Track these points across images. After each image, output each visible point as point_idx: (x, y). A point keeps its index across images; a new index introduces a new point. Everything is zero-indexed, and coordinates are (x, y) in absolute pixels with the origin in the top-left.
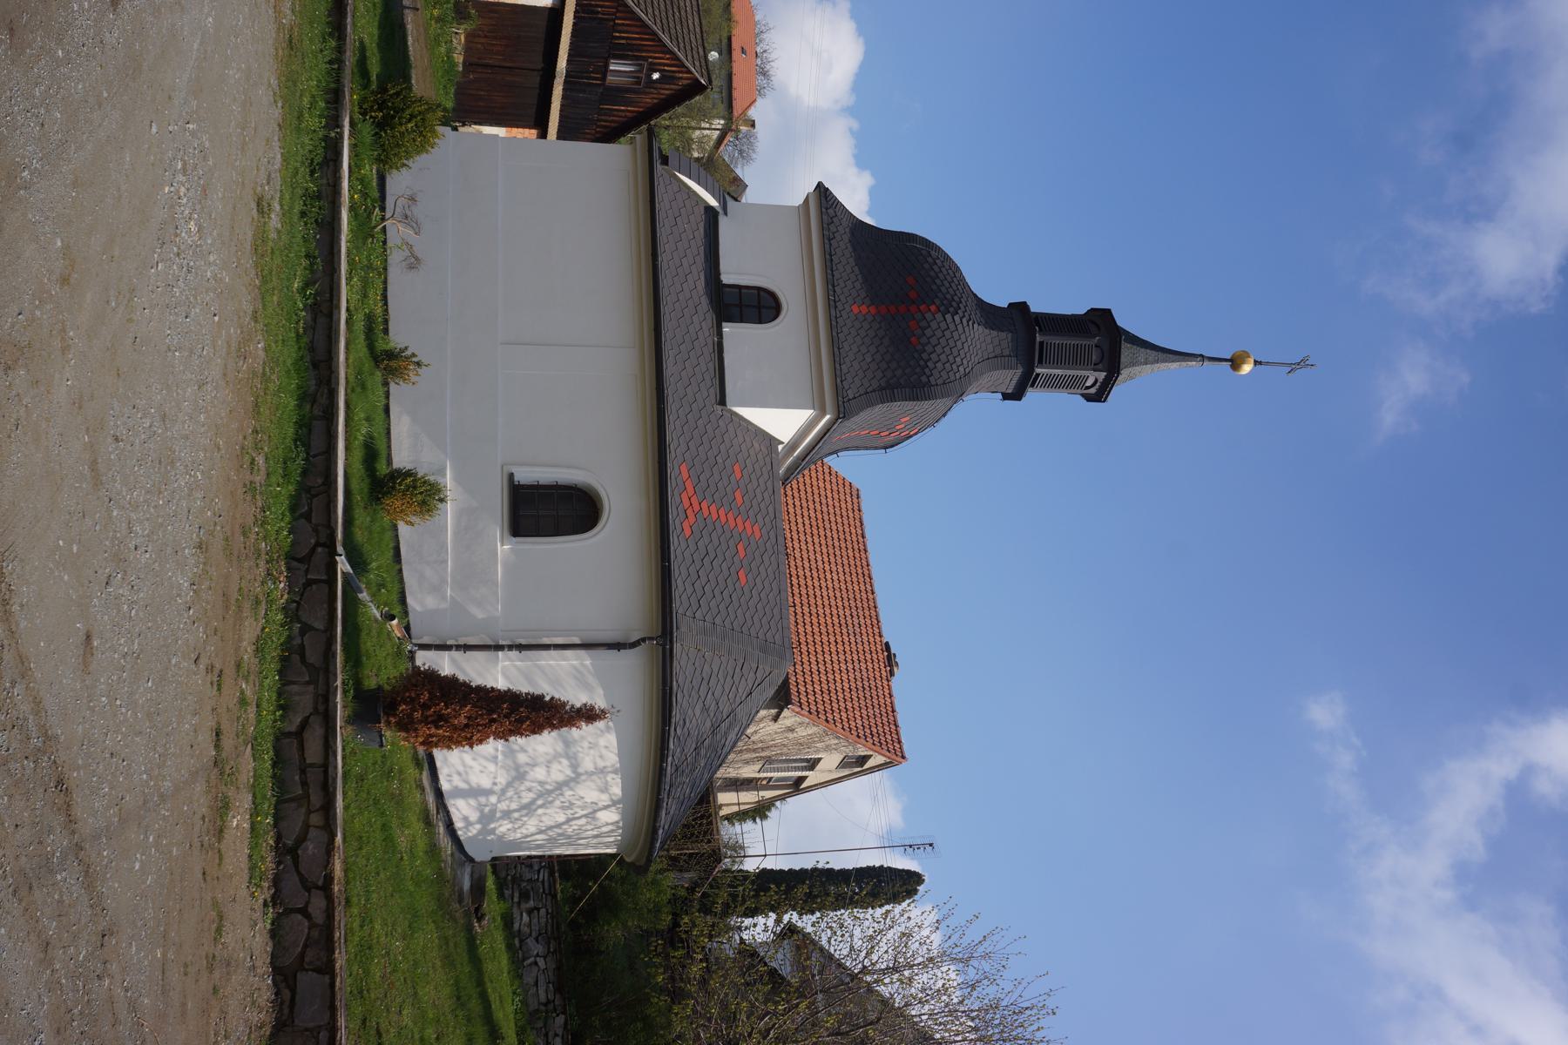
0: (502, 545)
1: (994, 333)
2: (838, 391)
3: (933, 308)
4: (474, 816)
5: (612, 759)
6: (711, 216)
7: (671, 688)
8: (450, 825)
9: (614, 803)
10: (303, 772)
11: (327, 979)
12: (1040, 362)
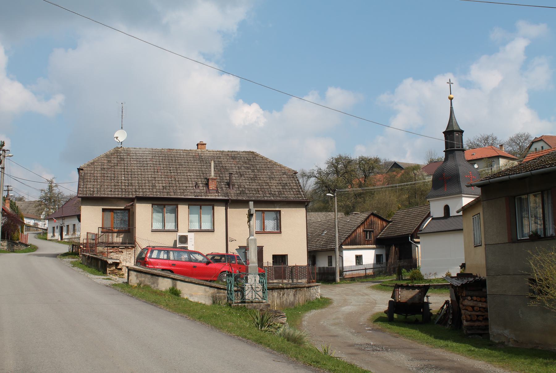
1: (449, 159)
2: (458, 194)
3: (444, 174)
6: (433, 219)
12: (454, 147)
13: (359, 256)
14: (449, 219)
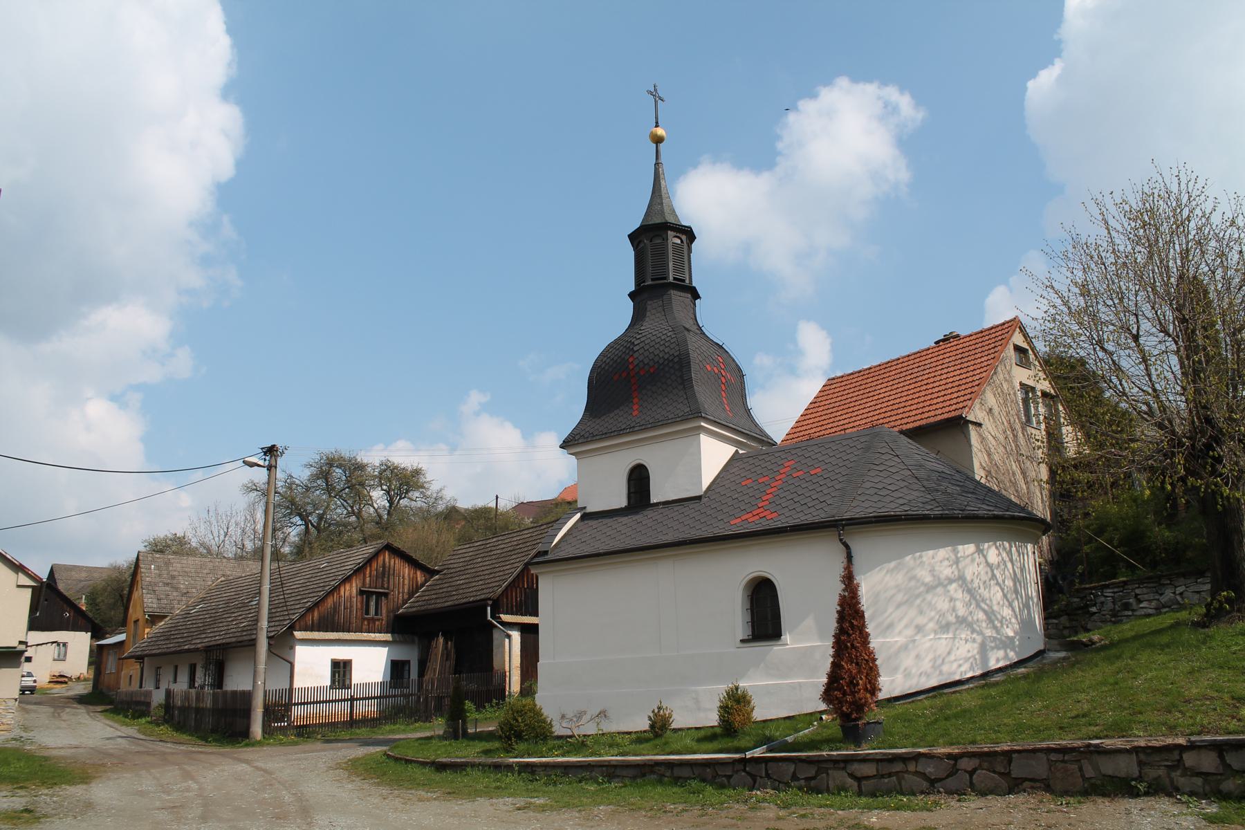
0: (787, 644)
1: (648, 314)
2: (685, 419)
3: (631, 360)
4: (1001, 653)
5: (943, 553)
6: (586, 517)
7: (875, 517)
9: (979, 551)
10: (883, 776)
11: (1014, 756)
12: (665, 278)
13: (342, 665)
14: (649, 513)
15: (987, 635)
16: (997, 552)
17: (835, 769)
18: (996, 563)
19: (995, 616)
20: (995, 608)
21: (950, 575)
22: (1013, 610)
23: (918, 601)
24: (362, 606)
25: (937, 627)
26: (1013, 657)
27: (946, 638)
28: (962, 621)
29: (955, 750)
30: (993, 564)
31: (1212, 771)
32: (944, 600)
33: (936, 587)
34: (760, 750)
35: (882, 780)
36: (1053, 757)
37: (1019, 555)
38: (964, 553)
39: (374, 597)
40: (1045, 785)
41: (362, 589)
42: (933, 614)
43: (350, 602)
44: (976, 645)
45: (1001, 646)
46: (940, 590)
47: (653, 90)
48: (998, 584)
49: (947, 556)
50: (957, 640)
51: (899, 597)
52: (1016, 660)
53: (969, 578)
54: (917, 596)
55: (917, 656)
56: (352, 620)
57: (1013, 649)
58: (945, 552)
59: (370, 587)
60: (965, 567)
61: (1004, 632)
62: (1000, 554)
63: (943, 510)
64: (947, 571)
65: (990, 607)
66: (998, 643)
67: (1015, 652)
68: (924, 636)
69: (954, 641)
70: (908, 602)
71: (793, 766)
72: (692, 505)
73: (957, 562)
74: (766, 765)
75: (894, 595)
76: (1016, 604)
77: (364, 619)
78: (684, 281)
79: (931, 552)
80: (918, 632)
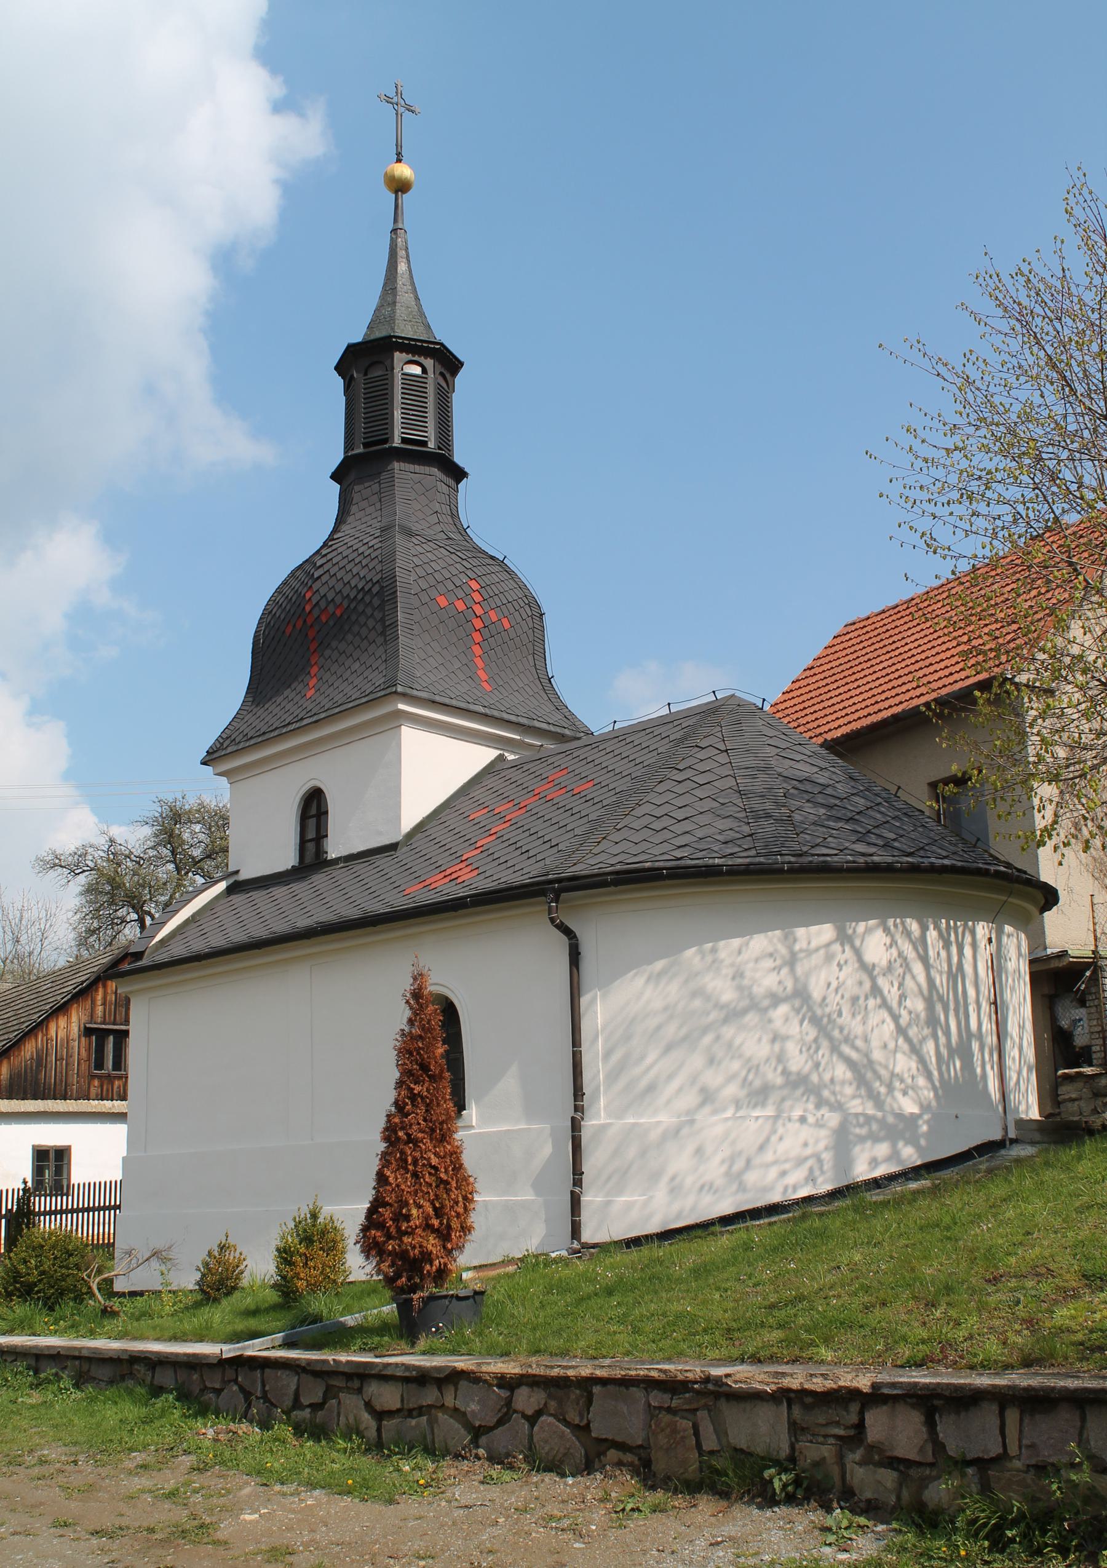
0: (472, 1127)
2: (373, 702)
4: (883, 1149)
5: (760, 943)
6: (236, 888)
7: (617, 873)
8: (876, 1184)
9: (844, 938)
10: (410, 1413)
11: (596, 1389)
13: (52, 1155)
14: (319, 879)
15: (853, 1111)
16: (888, 941)
17: (348, 1390)
18: (884, 963)
19: (875, 1072)
20: (877, 1055)
21: (775, 988)
22: (922, 1061)
23: (708, 1039)
24: (89, 1055)
25: (742, 1093)
26: (911, 1156)
27: (757, 1118)
28: (798, 1083)
29: (510, 1368)
30: (874, 965)
31: (913, 1455)
32: (760, 1040)
33: (745, 1011)
34: (263, 1343)
35: (409, 1420)
36: (657, 1398)
37: (947, 945)
38: (809, 943)
39: (111, 1038)
40: (640, 1459)
41: (88, 1025)
42: (736, 1065)
43: (67, 1048)
44: (823, 1133)
45: (882, 1134)
46: (751, 1018)
47: (392, 94)
48: (885, 1004)
49: (771, 949)
50: (780, 1122)
51: (671, 1031)
52: (919, 1163)
53: (816, 994)
54: (705, 1030)
55: (699, 1151)
56: (70, 1080)
57: (913, 1141)
58: (765, 942)
59: (104, 1023)
60: (807, 975)
61: (895, 1106)
62: (893, 943)
63: (758, 855)
64: (767, 981)
65: (867, 1055)
66: (875, 1127)
67: (918, 1147)
68: (715, 1112)
69: (775, 1123)
70: (688, 1040)
71: (297, 1377)
72: (382, 861)
73: (792, 961)
74: (262, 1374)
75: (659, 1028)
76: (929, 1047)
77: (93, 1077)
78: (424, 444)
79: (736, 942)
80: (703, 1104)
